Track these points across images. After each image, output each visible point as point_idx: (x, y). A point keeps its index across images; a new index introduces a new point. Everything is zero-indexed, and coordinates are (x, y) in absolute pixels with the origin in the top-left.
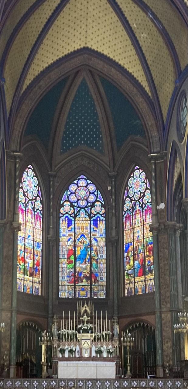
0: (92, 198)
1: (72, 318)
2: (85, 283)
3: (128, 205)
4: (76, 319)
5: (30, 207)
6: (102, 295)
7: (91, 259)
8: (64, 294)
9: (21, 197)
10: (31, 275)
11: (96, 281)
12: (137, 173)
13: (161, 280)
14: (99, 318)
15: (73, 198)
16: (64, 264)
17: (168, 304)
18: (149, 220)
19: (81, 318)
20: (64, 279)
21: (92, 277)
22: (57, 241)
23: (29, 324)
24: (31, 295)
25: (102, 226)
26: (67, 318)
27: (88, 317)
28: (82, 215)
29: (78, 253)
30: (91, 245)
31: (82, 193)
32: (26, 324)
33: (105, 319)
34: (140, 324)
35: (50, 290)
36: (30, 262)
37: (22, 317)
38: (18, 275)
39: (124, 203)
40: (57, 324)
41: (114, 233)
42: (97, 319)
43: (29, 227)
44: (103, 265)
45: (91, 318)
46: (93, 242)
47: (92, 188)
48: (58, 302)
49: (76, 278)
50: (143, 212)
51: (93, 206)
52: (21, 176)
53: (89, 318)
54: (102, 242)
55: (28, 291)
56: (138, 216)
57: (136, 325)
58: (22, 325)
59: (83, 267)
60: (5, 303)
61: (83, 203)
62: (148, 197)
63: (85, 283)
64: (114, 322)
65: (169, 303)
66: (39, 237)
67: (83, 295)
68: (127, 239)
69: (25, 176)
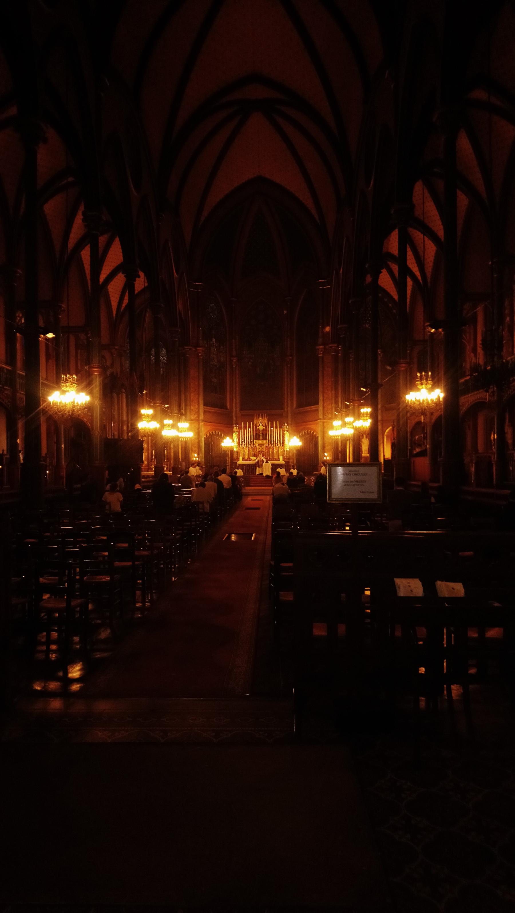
1: (250, 427)
4: (253, 428)
13: (325, 395)
14: (272, 426)
17: (329, 414)
19: (257, 428)
23: (215, 433)
26: (245, 428)
27: (263, 427)
32: (212, 433)
33: (277, 428)
34: (308, 432)
35: (234, 405)
40: (237, 433)
42: (279, 428)
45: (266, 426)
48: (241, 414)
53: (265, 428)
57: (305, 432)
58: (210, 434)
60: (193, 416)
64: (284, 431)
65: (330, 414)
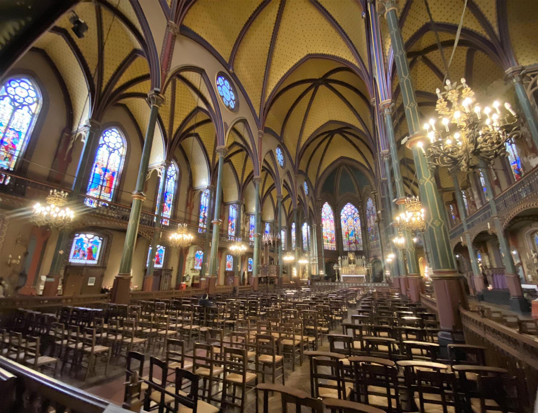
0: (353, 211)
2: (353, 245)
3: (368, 212)
5: (328, 218)
6: (361, 249)
7: (355, 235)
8: (345, 249)
9: (323, 214)
10: (331, 242)
11: (358, 244)
12: (369, 199)
15: (346, 212)
16: (344, 238)
18: (376, 218)
20: (345, 243)
21: (356, 242)
22: (340, 229)
24: (332, 250)
25: (359, 222)
28: (350, 218)
29: (350, 233)
30: (355, 230)
31: (349, 210)
36: (330, 238)
37: (327, 259)
38: (324, 243)
39: (366, 212)
41: (363, 224)
43: (328, 225)
44: (360, 237)
46: (356, 229)
47: (353, 207)
49: (350, 243)
50: (373, 215)
51: (354, 214)
52: (322, 207)
54: (359, 228)
55: (330, 249)
56: (372, 217)
59: (352, 238)
61: (350, 214)
62: (374, 209)
63: (353, 245)
66: (333, 228)
67: (353, 249)
68: (369, 225)
69: (324, 206)
